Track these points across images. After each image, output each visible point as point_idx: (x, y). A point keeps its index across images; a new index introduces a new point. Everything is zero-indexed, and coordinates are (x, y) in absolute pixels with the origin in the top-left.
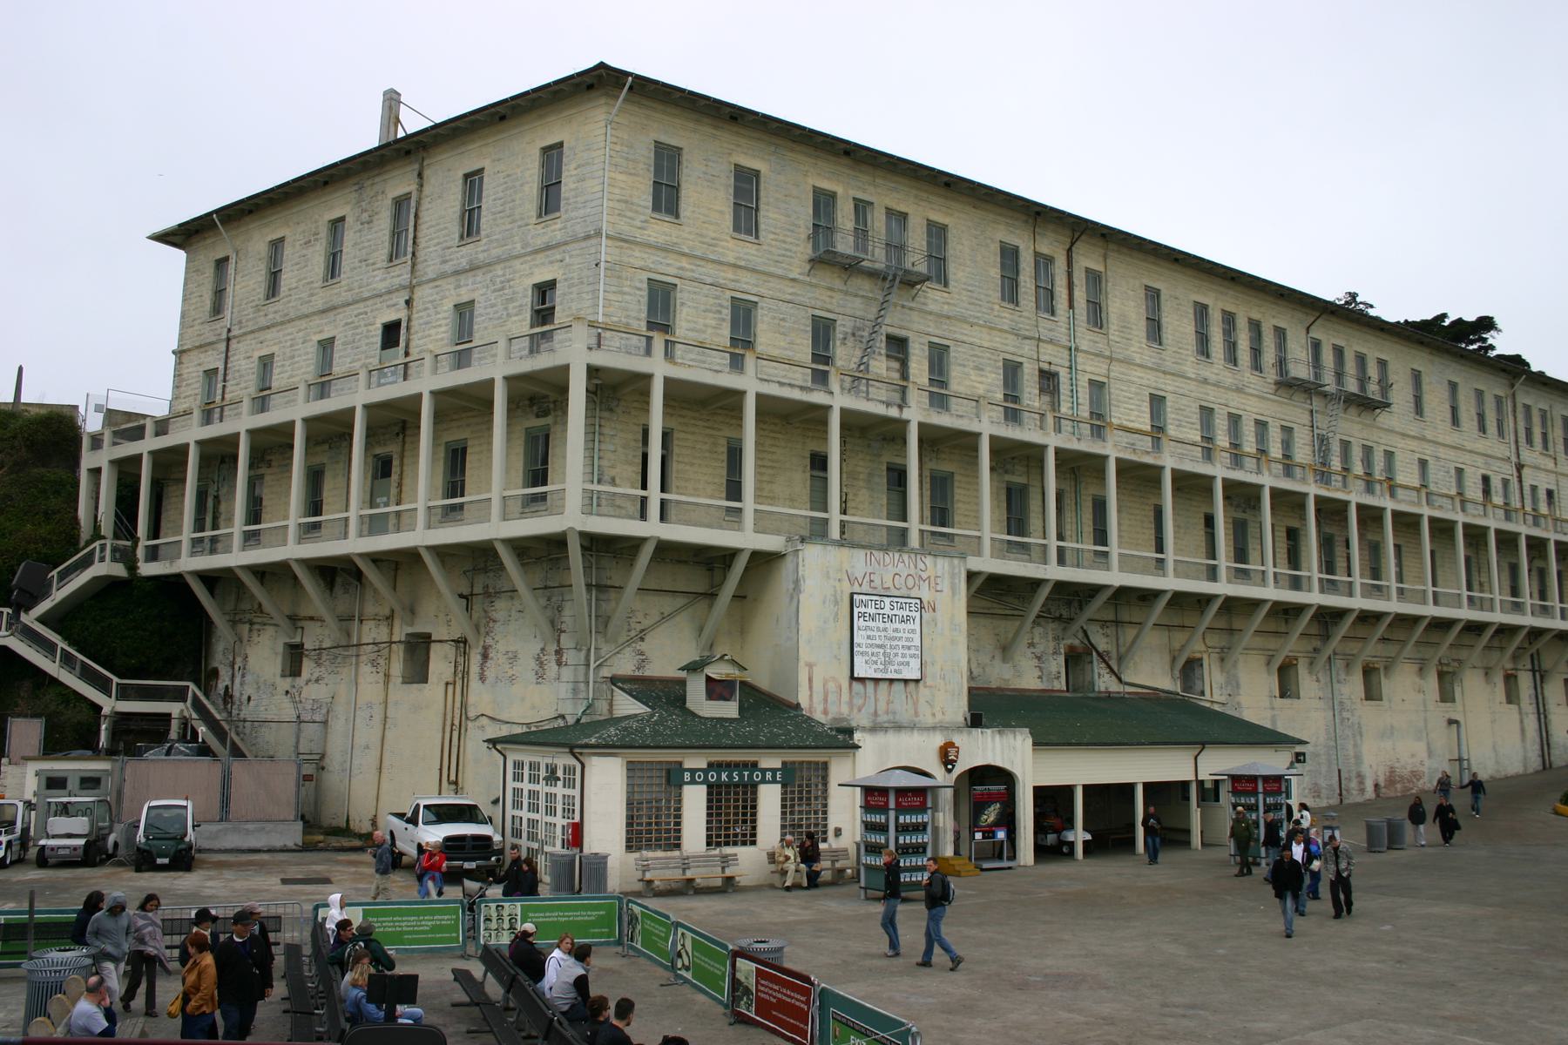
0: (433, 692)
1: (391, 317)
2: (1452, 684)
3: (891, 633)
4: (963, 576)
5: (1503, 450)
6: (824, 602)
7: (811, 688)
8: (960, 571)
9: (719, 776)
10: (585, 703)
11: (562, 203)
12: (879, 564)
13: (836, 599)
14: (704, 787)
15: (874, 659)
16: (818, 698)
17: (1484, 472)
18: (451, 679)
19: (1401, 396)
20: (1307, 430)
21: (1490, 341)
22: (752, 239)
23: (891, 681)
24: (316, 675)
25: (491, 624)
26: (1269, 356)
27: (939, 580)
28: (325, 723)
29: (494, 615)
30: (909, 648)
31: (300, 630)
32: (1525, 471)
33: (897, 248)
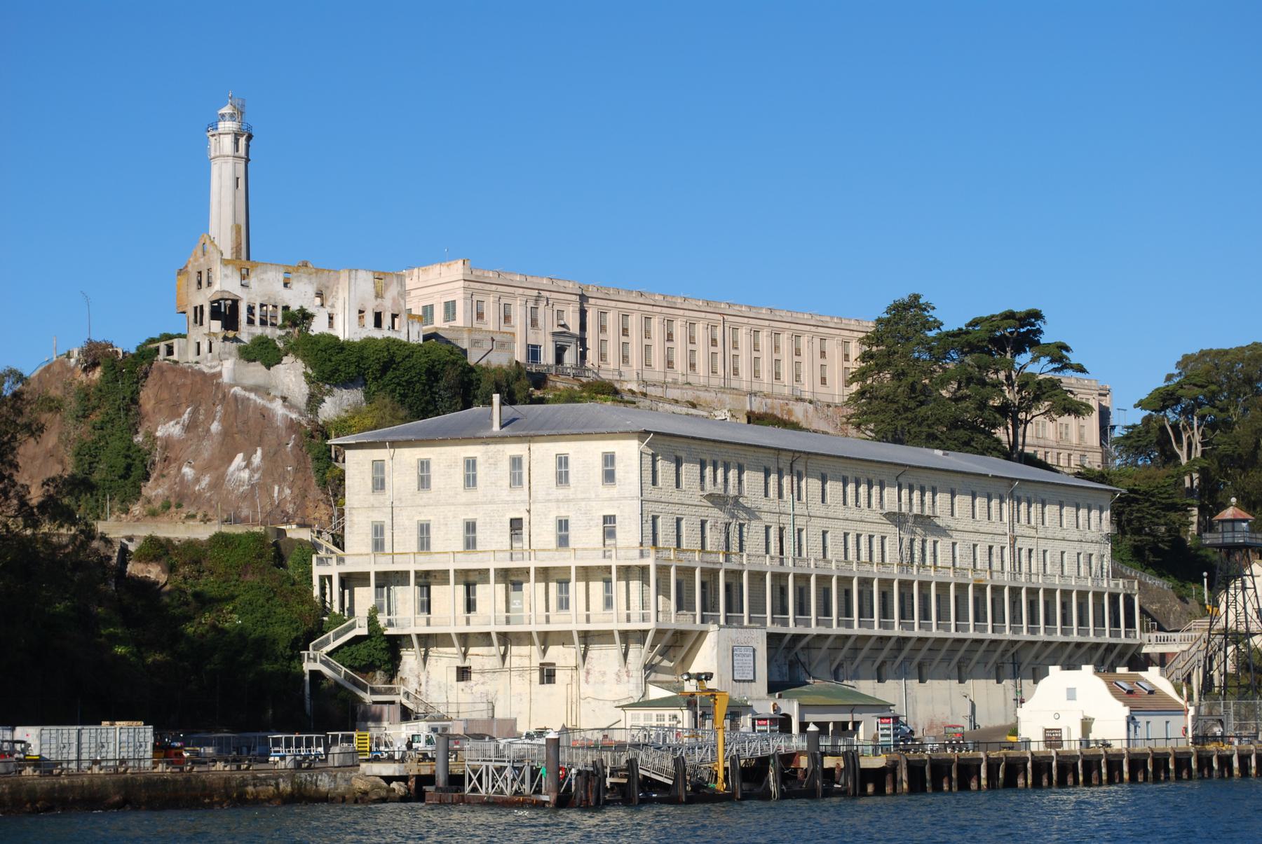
1: (518, 516)
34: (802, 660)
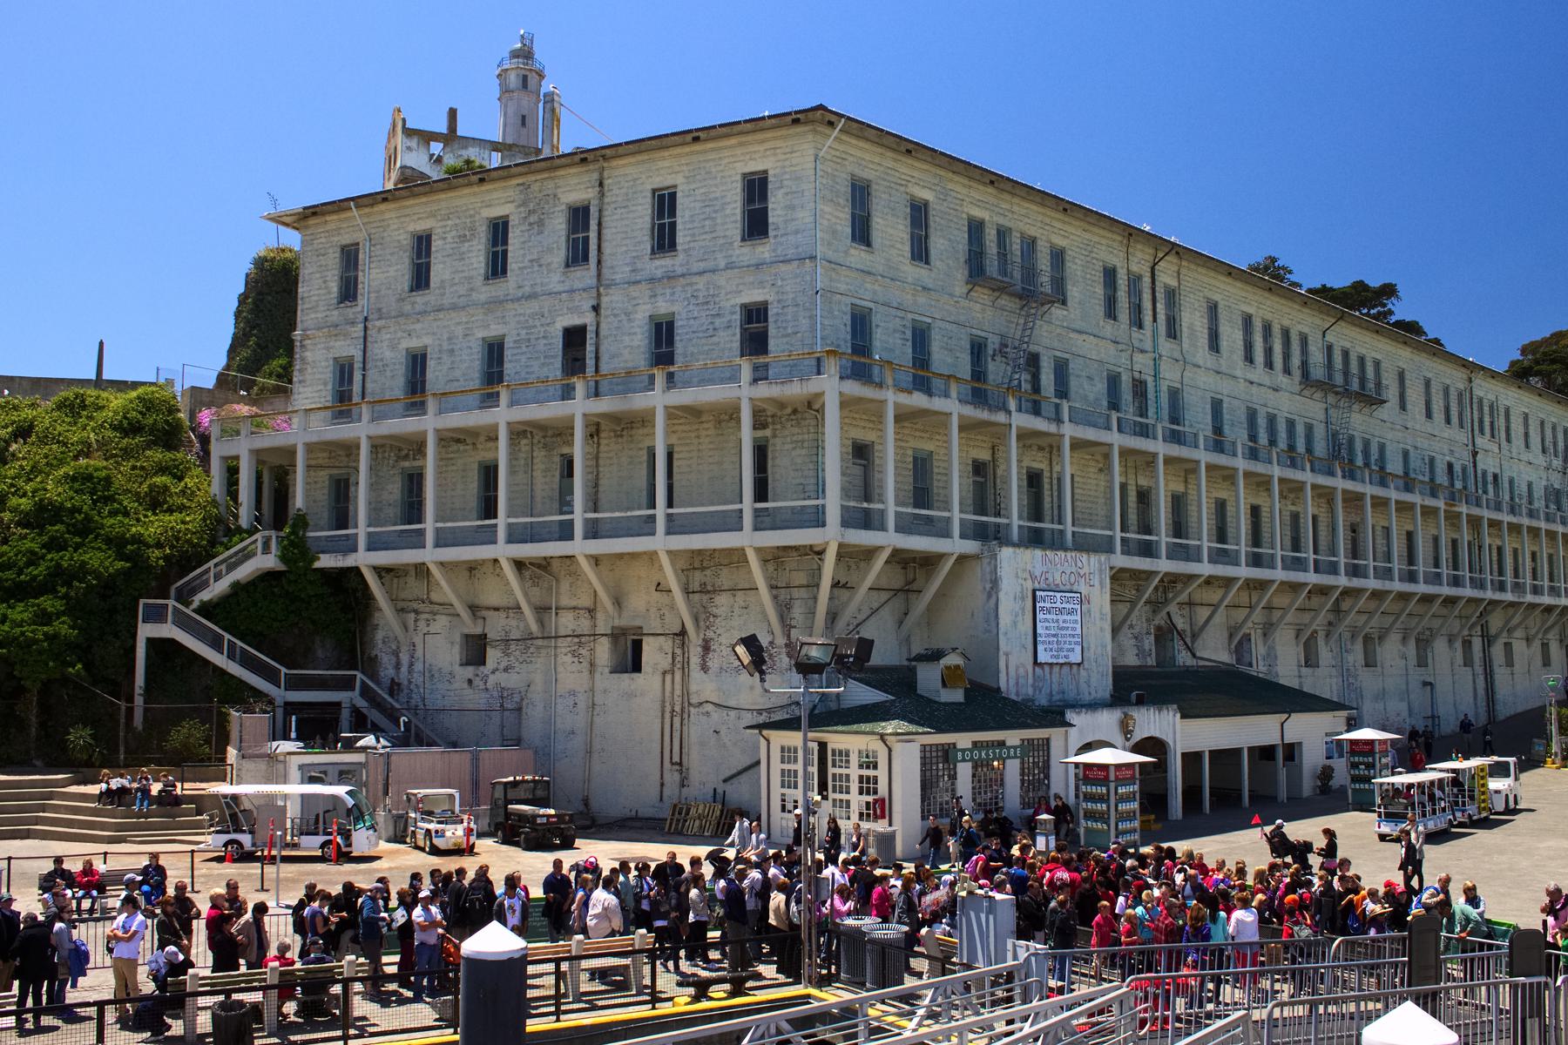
1: (576, 321)
2: (1425, 650)
3: (1062, 624)
5: (1462, 437)
11: (771, 228)
14: (970, 764)
16: (1012, 682)
17: (1448, 458)
18: (668, 667)
19: (1392, 393)
20: (1323, 425)
21: (1390, 306)
22: (922, 265)
23: (1062, 665)
25: (711, 619)
26: (1296, 361)
28: (519, 709)
29: (715, 611)
30: (1073, 636)
32: (1479, 457)
33: (1030, 273)
34: (1180, 626)
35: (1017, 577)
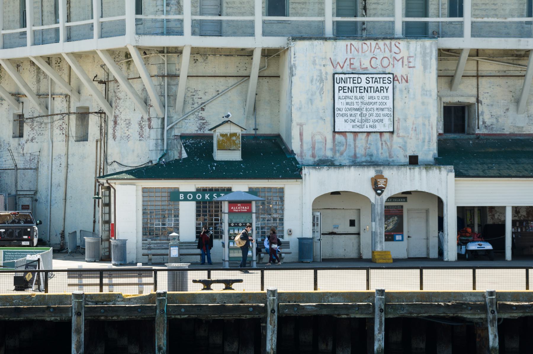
0: (90, 147)
3: (366, 100)
4: (435, 53)
6: (312, 81)
7: (301, 140)
8: (431, 51)
9: (204, 196)
10: (162, 153)
12: (358, 51)
13: (321, 76)
14: (194, 204)
15: (353, 118)
23: (369, 133)
24: (31, 136)
27: (411, 60)
28: (36, 169)
30: (382, 110)
31: (21, 104)
35: (314, 63)
